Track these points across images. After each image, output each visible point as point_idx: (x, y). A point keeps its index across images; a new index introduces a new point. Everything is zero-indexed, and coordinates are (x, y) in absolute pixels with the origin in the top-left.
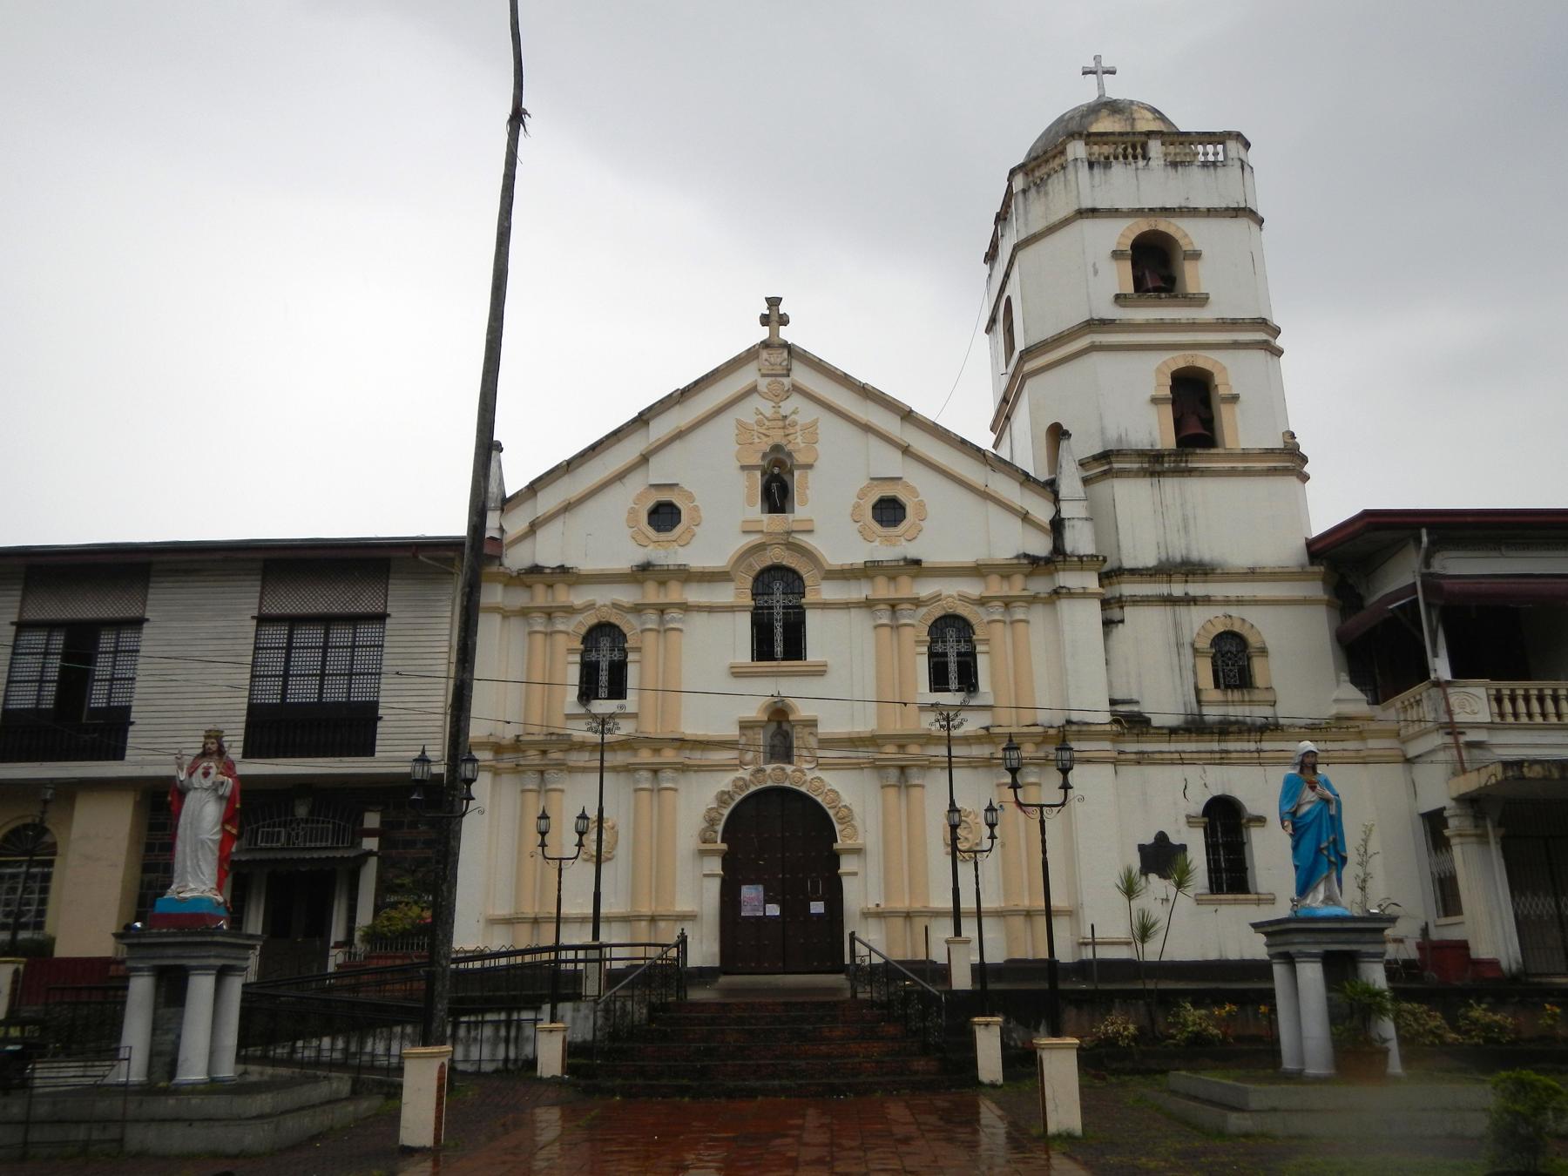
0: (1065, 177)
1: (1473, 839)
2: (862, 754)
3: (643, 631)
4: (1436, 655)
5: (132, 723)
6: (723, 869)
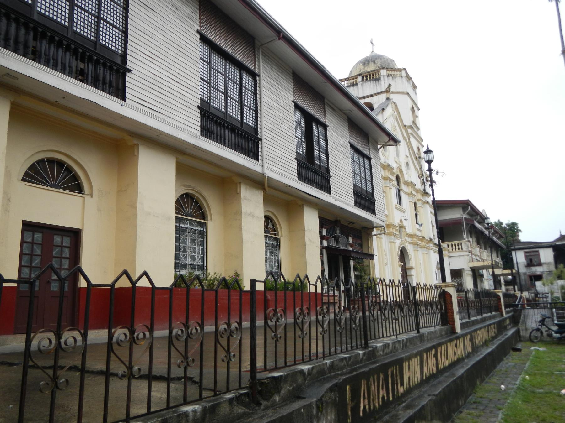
0: (402, 80)
1: (470, 276)
2: (409, 240)
3: (385, 187)
4: (465, 234)
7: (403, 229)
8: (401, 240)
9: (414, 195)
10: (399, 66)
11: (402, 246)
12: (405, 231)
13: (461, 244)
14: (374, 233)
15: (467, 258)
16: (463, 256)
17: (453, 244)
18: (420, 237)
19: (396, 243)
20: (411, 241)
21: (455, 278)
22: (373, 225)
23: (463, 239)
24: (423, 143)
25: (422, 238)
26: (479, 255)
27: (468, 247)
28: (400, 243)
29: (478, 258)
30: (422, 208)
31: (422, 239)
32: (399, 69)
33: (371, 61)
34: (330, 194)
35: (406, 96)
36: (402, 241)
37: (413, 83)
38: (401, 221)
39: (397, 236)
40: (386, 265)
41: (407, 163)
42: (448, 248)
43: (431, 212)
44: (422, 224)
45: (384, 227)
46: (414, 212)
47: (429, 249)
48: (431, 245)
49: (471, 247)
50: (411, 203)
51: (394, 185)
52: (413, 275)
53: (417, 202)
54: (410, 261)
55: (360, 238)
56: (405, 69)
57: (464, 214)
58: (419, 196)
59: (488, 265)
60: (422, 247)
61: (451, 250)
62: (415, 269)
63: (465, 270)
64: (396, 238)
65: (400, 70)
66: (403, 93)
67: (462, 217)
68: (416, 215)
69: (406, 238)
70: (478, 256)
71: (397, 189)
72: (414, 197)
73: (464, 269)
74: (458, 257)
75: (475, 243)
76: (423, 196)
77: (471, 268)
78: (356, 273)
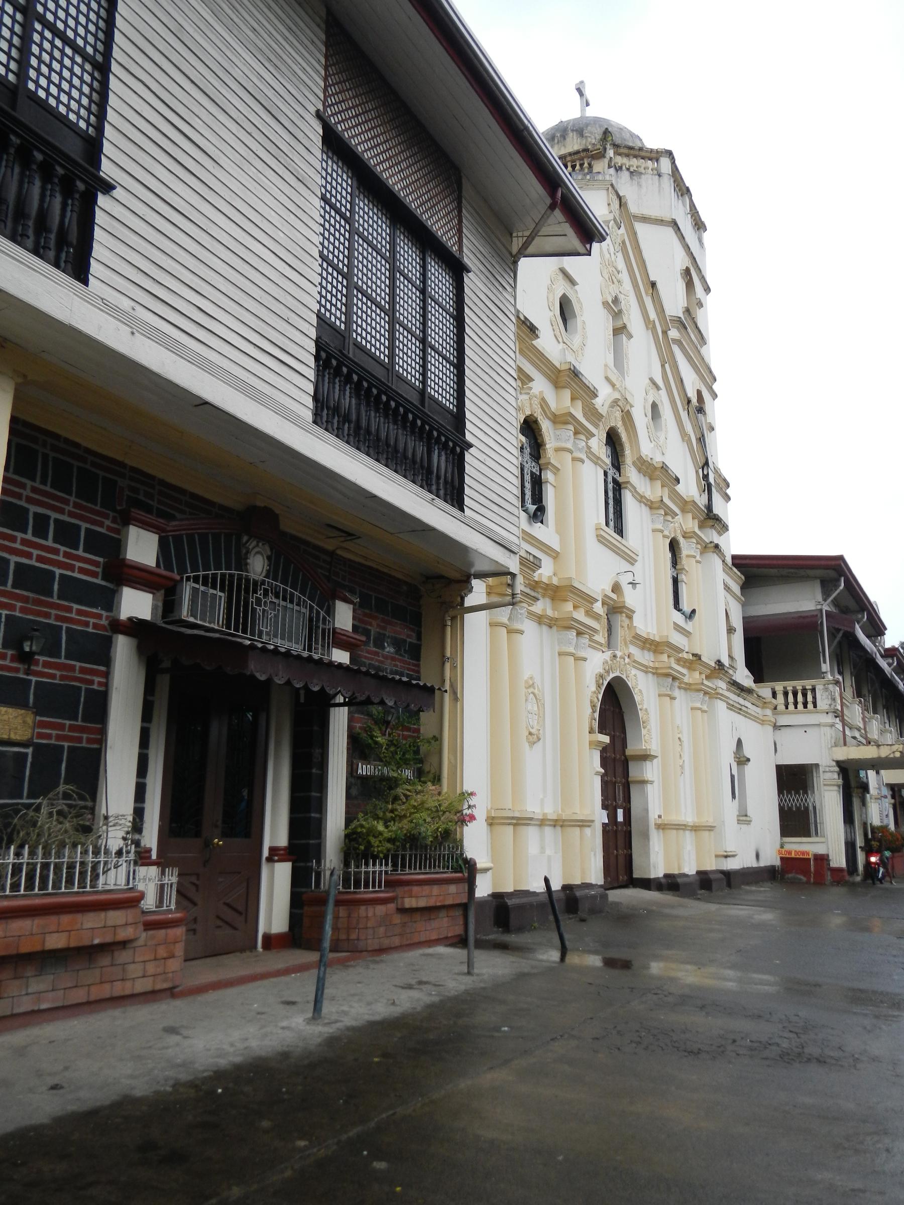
1: (836, 788)
2: (645, 657)
4: (825, 662)
5: (108, 188)
6: (603, 765)
7: (621, 620)
8: (608, 655)
9: (669, 512)
10: (651, 143)
11: (612, 676)
12: (631, 627)
13: (813, 690)
14: (470, 601)
15: (828, 735)
16: (819, 725)
17: (790, 689)
18: (685, 656)
19: (585, 659)
20: (651, 664)
21: (789, 792)
22: (471, 565)
23: (820, 675)
24: (715, 387)
25: (691, 657)
26: (862, 726)
27: (834, 700)
28: (605, 662)
29: (857, 734)
30: (698, 562)
31: (691, 662)
32: (652, 151)
33: (573, 131)
34: (85, 282)
35: (670, 231)
36: (615, 656)
37: (693, 206)
38: (616, 588)
39: (591, 636)
40: (534, 738)
41: (654, 406)
42: (773, 700)
43: (727, 588)
44: (694, 611)
45: (513, 576)
46: (667, 573)
47: (711, 695)
48: (722, 685)
49: (842, 704)
50: (661, 535)
51: (596, 460)
52: (652, 782)
53: (682, 540)
54: (644, 732)
55: (415, 621)
56: (670, 154)
57: (825, 600)
58: (691, 524)
59: (892, 756)
60: (688, 688)
61: (781, 707)
62: (660, 758)
63: (821, 769)
64: (585, 640)
65: (655, 156)
66: (660, 222)
67: (821, 610)
68: (675, 581)
69: (633, 650)
70: (859, 729)
71: (610, 479)
72: (669, 518)
73: (817, 765)
74: (802, 730)
75: (849, 693)
76: (701, 526)
77: (839, 763)
78: (364, 769)
